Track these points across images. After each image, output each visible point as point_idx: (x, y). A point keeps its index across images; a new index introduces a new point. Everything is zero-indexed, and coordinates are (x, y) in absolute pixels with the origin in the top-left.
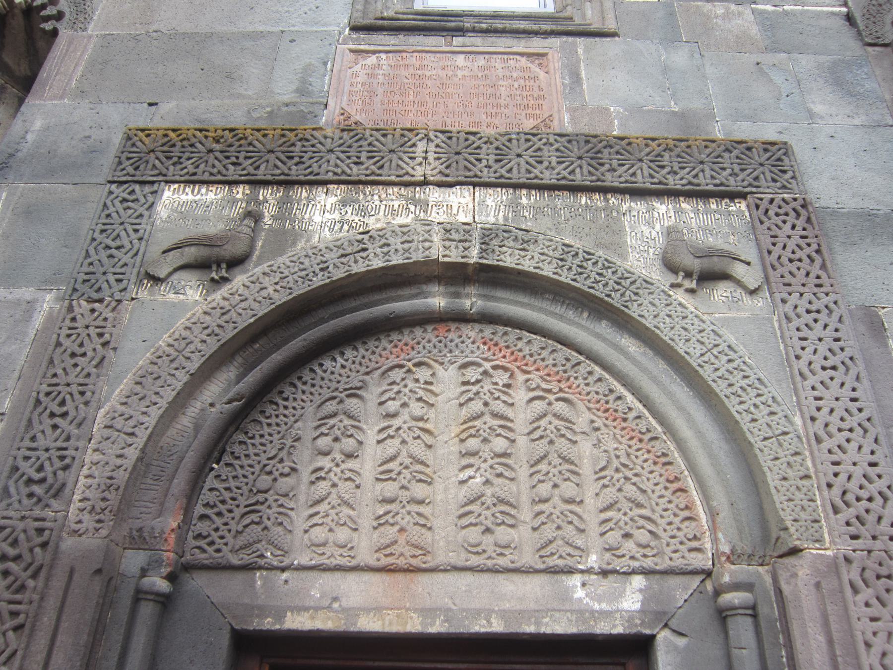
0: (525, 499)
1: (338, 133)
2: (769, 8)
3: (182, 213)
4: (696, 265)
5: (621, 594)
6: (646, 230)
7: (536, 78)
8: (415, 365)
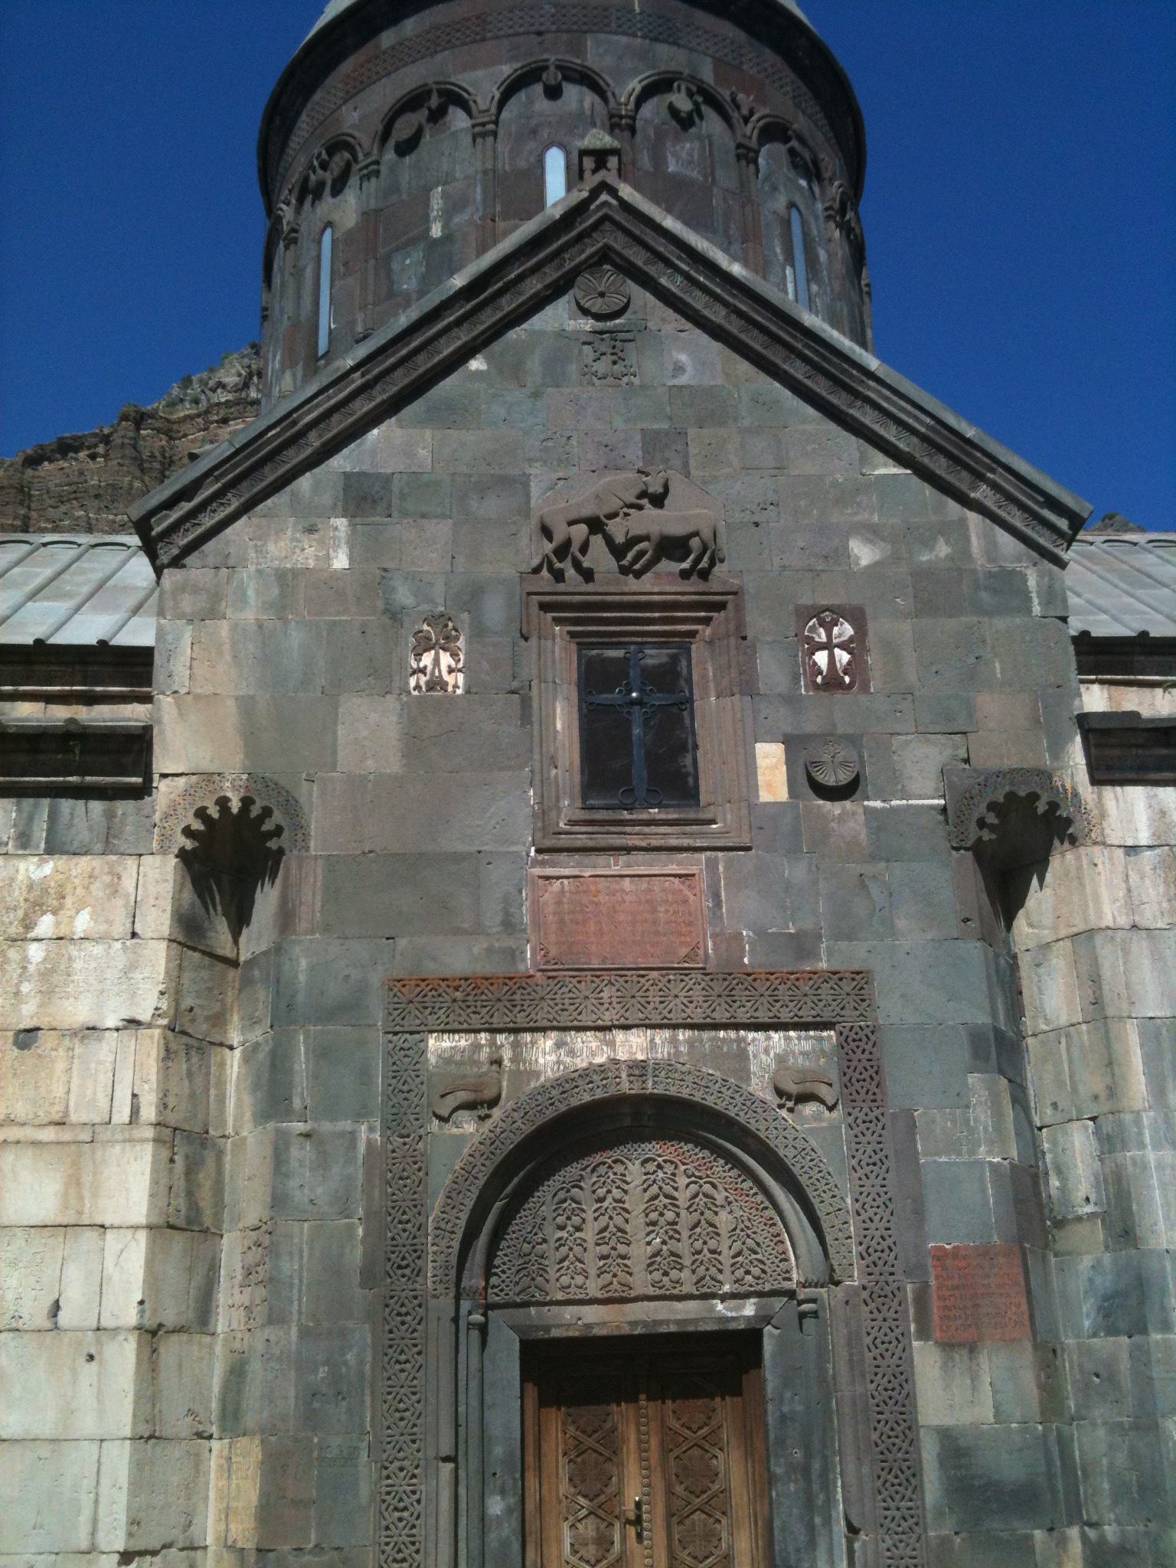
0: (686, 1252)
1: (545, 982)
2: (878, 804)
3: (447, 1060)
4: (793, 1089)
5: (744, 1306)
6: (763, 1057)
7: (685, 901)
8: (615, 1162)
